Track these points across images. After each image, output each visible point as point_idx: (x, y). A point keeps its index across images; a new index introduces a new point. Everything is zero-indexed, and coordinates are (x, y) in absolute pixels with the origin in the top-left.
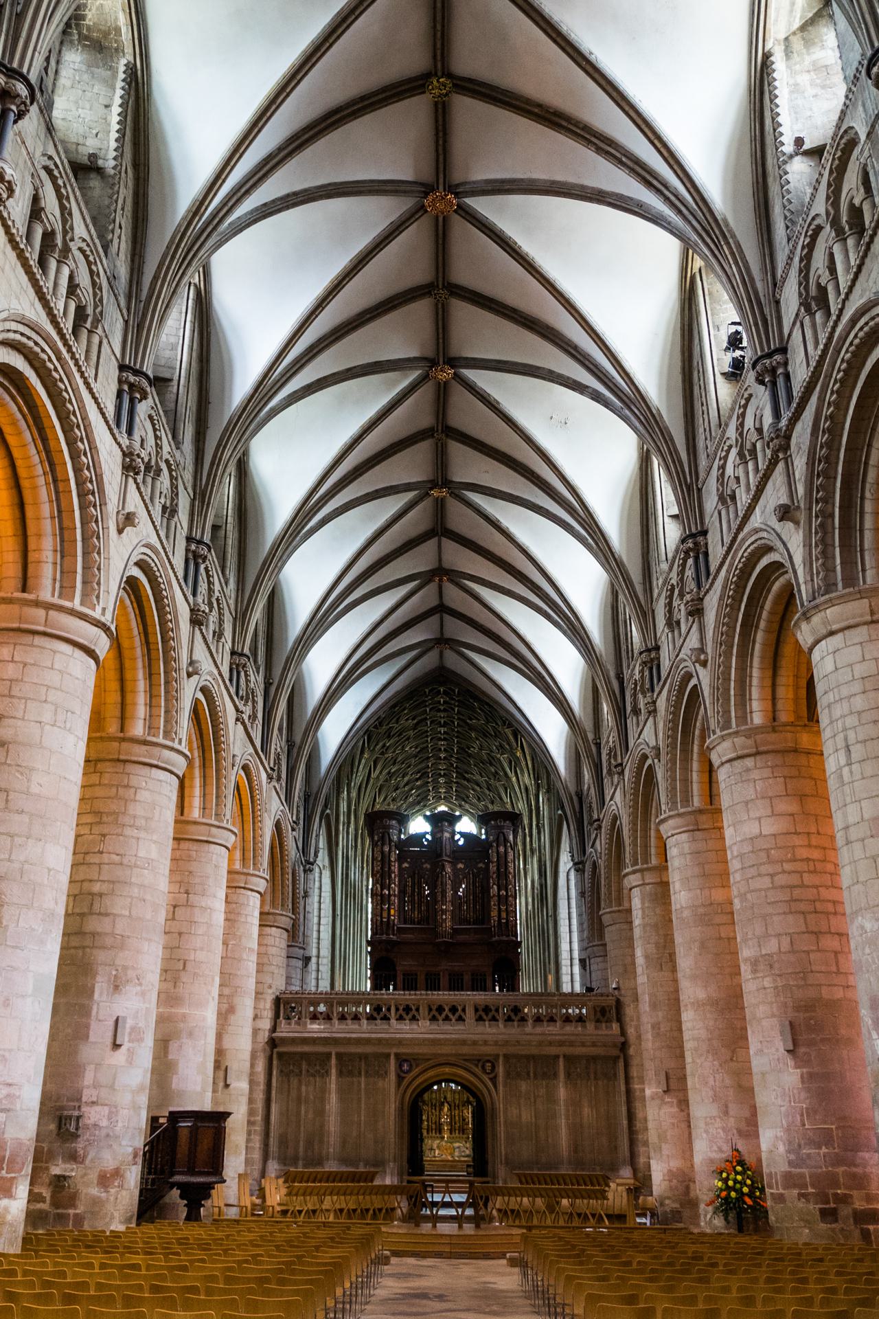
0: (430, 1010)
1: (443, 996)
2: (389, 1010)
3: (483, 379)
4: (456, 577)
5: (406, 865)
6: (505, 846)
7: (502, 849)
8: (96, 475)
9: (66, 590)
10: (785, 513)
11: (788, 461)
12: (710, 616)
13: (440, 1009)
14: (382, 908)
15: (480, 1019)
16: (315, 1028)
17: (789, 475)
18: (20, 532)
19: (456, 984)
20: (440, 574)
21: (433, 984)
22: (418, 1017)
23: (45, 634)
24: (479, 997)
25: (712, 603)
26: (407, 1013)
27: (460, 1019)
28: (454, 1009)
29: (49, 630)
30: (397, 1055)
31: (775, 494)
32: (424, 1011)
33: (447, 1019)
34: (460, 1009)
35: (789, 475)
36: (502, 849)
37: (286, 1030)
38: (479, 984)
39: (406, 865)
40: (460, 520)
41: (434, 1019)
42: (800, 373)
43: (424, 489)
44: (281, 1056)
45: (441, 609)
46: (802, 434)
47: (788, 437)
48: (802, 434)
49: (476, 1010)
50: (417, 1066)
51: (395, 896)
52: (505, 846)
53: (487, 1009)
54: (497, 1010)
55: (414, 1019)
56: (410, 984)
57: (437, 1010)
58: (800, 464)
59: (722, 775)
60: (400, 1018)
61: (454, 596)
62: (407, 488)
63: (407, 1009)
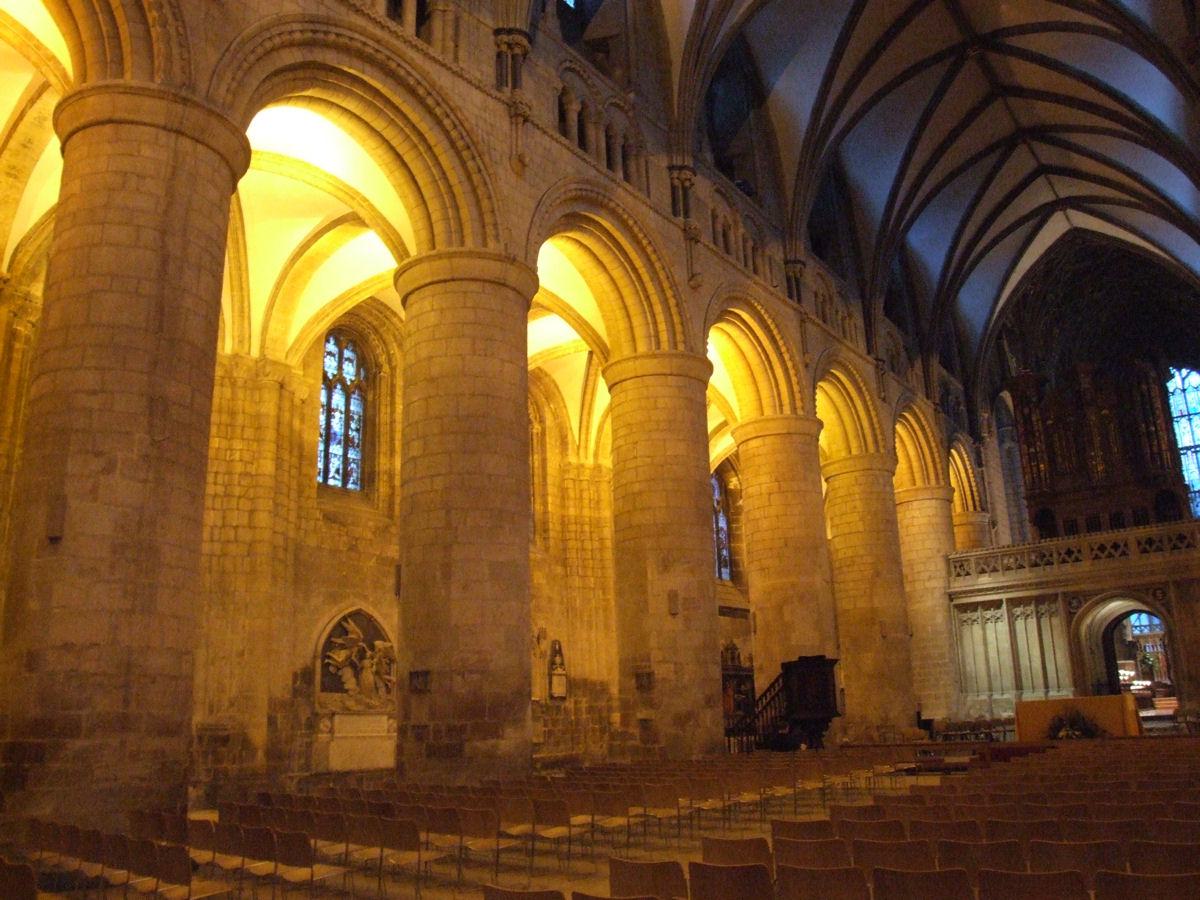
0: (1092, 550)
2: (1051, 555)
5: (1050, 422)
6: (1148, 384)
7: (1144, 387)
8: (466, 131)
13: (1102, 548)
14: (1031, 466)
15: (1145, 551)
16: (985, 581)
18: (420, 201)
19: (1117, 522)
21: (1094, 526)
22: (1080, 558)
23: (453, 280)
24: (1142, 532)
27: (1124, 553)
28: (1116, 546)
29: (456, 276)
30: (1064, 593)
32: (1086, 551)
33: (1110, 556)
34: (1122, 545)
36: (1144, 387)
37: (959, 585)
38: (1140, 520)
39: (1050, 422)
41: (1097, 557)
43: (955, 56)
44: (956, 606)
49: (1139, 543)
50: (1086, 601)
51: (1042, 452)
52: (1148, 384)
53: (1150, 541)
54: (1161, 541)
55: (1077, 560)
56: (1072, 529)
57: (1099, 549)
60: (1064, 561)
62: (937, 58)
63: (1069, 552)
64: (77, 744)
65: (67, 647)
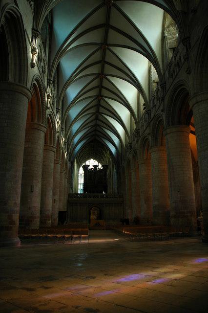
1: (96, 194)
3: (107, 100)
4: (99, 125)
9: (51, 143)
10: (149, 134)
11: (150, 126)
12: (139, 142)
17: (150, 128)
20: (96, 125)
25: (139, 141)
26: (90, 197)
31: (147, 131)
35: (150, 128)
40: (100, 117)
42: (152, 117)
43: (93, 114)
45: (95, 130)
46: (151, 124)
47: (150, 123)
48: (151, 124)
58: (151, 128)
59: (139, 166)
61: (98, 128)
62: (91, 113)
64: (36, 220)
65: (34, 207)
